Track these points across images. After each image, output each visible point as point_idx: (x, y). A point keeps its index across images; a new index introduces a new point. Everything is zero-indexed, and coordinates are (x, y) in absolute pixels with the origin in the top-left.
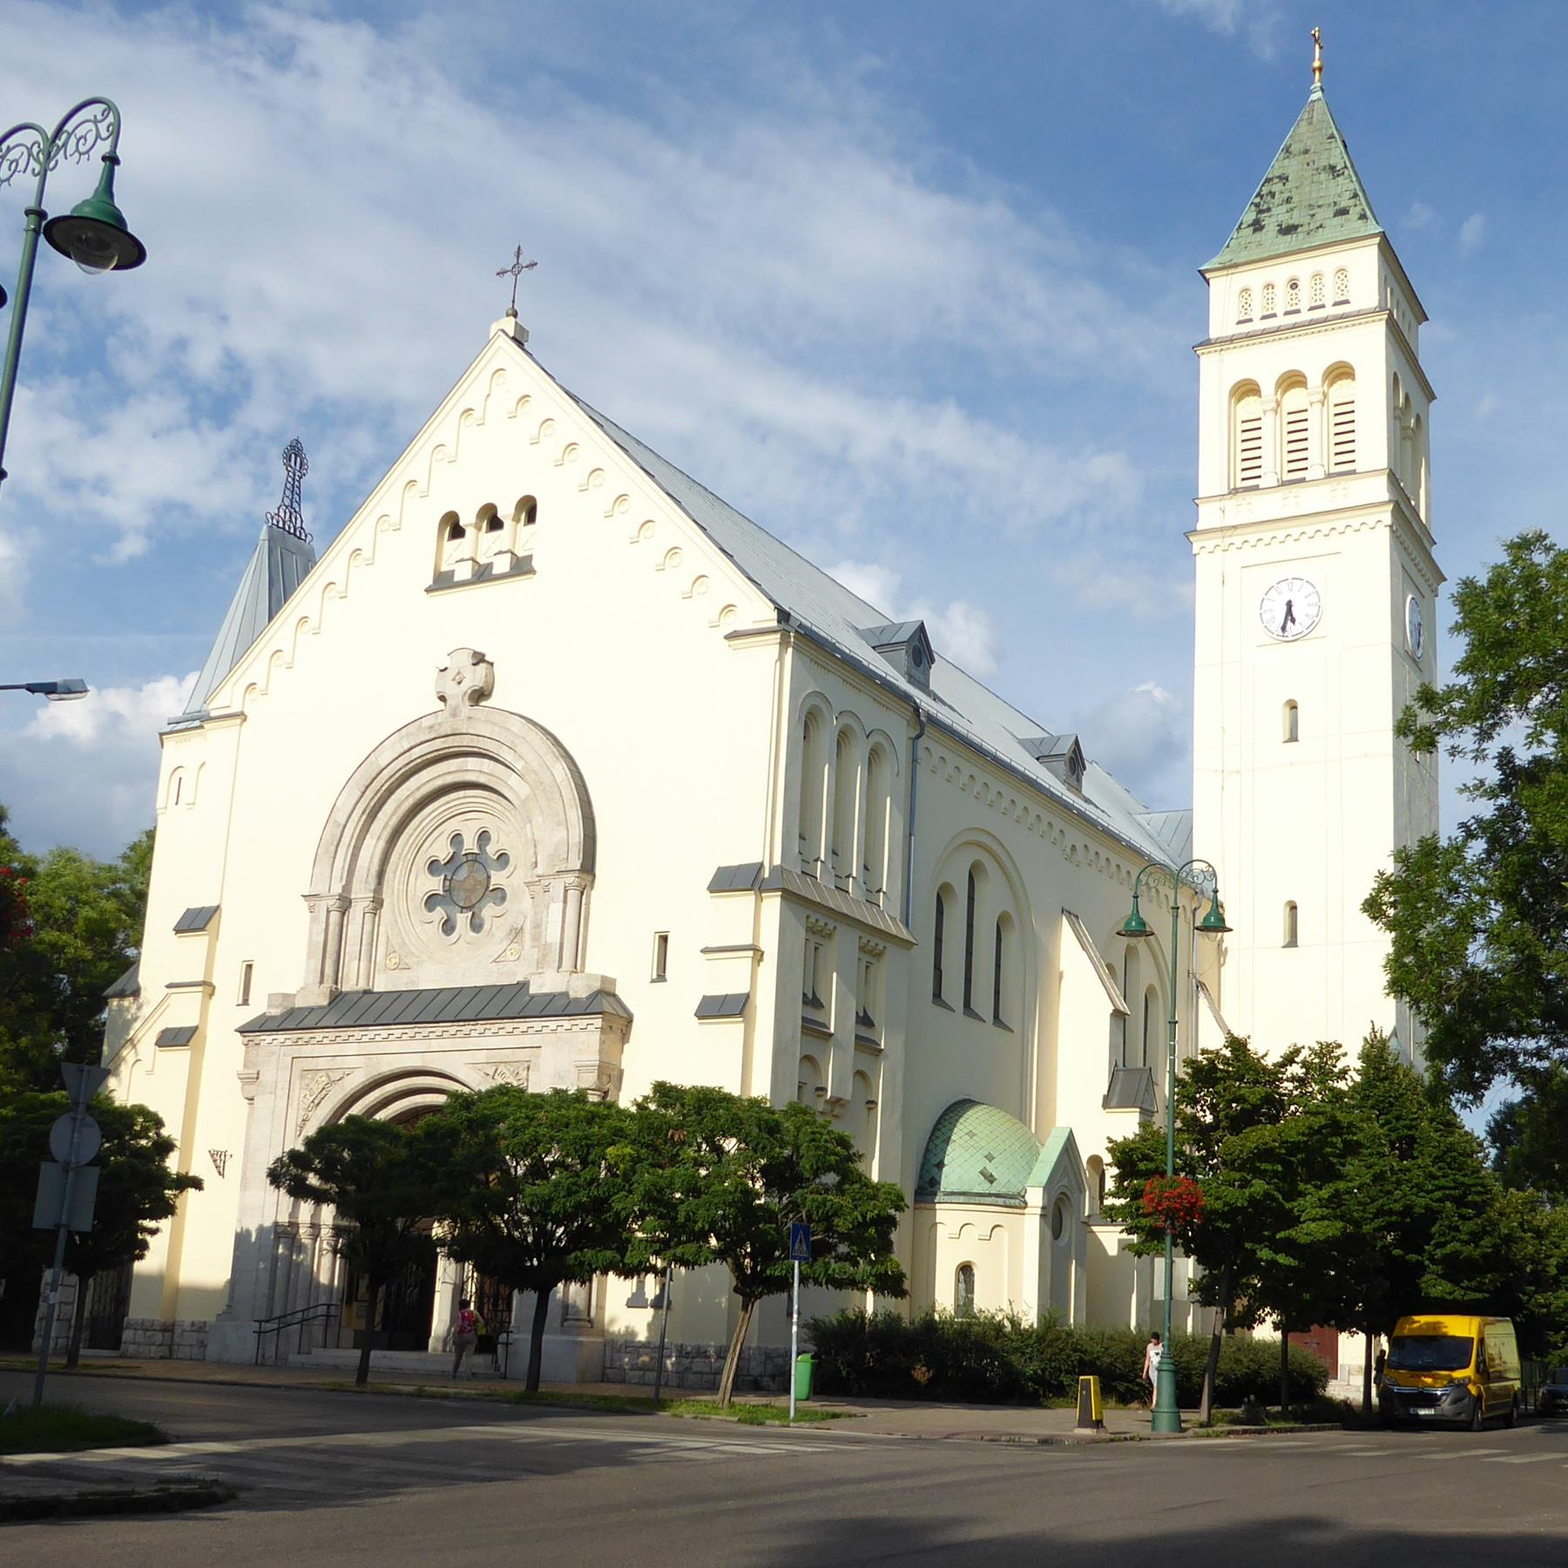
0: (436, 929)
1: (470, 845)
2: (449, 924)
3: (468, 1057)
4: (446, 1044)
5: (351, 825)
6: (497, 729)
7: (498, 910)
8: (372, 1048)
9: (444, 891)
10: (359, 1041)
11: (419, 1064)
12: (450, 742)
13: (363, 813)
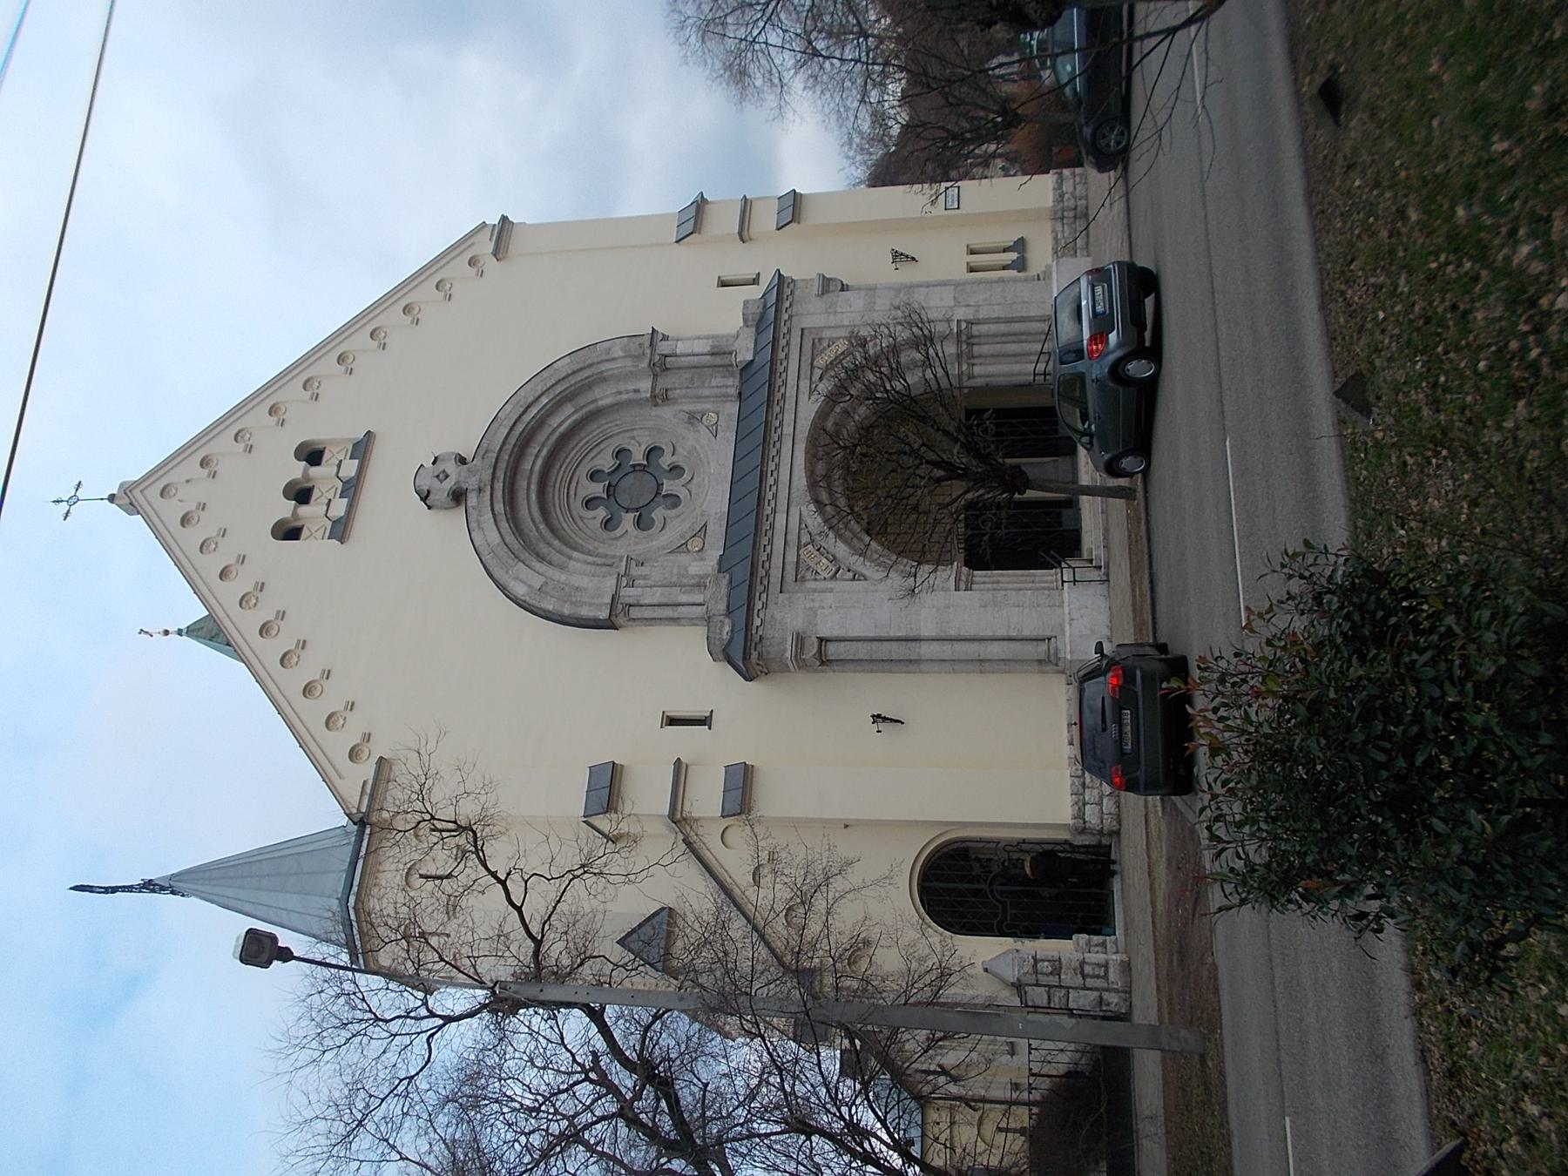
1: (598, 489)
3: (804, 397)
4: (789, 417)
7: (668, 450)
8: (783, 494)
10: (774, 511)
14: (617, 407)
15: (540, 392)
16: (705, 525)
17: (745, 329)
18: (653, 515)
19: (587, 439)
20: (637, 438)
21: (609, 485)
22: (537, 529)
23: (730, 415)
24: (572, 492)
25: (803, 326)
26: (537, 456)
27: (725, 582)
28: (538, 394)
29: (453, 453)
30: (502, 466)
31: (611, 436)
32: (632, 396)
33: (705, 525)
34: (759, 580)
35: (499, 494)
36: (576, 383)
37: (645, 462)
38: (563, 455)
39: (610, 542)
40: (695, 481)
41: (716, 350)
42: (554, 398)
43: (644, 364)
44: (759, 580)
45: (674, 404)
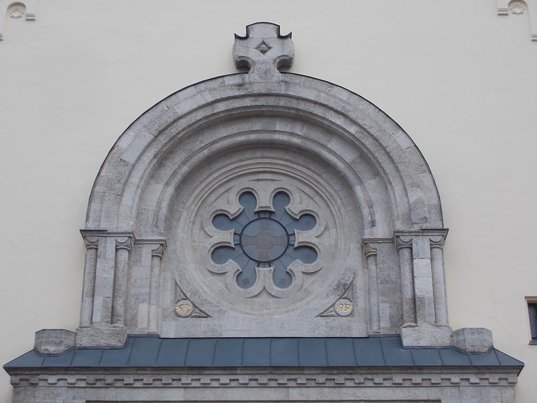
0: (231, 279)
2: (244, 276)
5: (141, 168)
6: (322, 95)
7: (310, 267)
9: (235, 245)
10: (186, 387)
12: (261, 101)
13: (155, 157)
14: (357, 207)
15: (361, 123)
16: (207, 316)
17: (449, 334)
18: (230, 260)
19: (322, 182)
20: (327, 234)
21: (271, 213)
22: (202, 148)
23: (349, 328)
24: (261, 176)
26: (292, 134)
27: (114, 342)
28: (359, 121)
29: (293, 55)
30: (271, 101)
31: (328, 206)
32: (367, 218)
33: (207, 316)
34: (100, 377)
35: (237, 104)
36: (376, 158)
37: (296, 245)
38: (301, 161)
39: (198, 221)
40: (271, 300)
41: (418, 303)
42: (358, 140)
43: (399, 226)
44: (100, 377)
45: (363, 266)
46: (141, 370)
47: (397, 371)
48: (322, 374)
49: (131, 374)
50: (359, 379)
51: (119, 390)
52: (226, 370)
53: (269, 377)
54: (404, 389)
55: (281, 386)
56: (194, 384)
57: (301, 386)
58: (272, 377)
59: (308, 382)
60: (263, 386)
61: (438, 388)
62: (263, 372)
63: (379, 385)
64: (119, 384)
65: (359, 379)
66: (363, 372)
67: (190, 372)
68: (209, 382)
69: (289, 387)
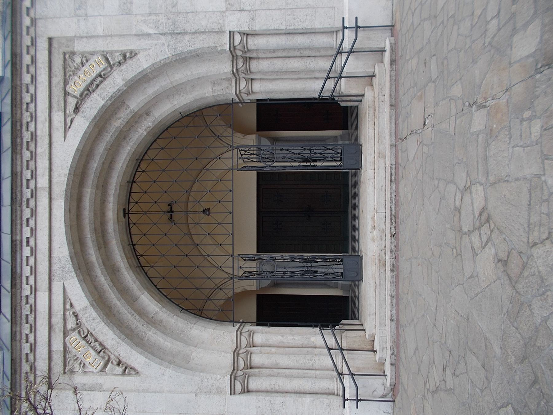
3: (58, 135)
4: (42, 164)
11: (63, 204)
25: (51, 35)
46: (16, 337)
47: (19, 79)
48: (21, 154)
49: (21, 346)
50: (26, 117)
51: (38, 356)
52: (16, 251)
53: (24, 207)
54: (38, 73)
55: (34, 194)
56: (32, 281)
57: (34, 175)
58: (24, 204)
59: (30, 168)
60: (34, 213)
61: (38, 40)
62: (19, 212)
63: (34, 98)
64: (31, 357)
65: (26, 117)
66: (19, 113)
67: (18, 287)
68: (29, 267)
69: (36, 187)
